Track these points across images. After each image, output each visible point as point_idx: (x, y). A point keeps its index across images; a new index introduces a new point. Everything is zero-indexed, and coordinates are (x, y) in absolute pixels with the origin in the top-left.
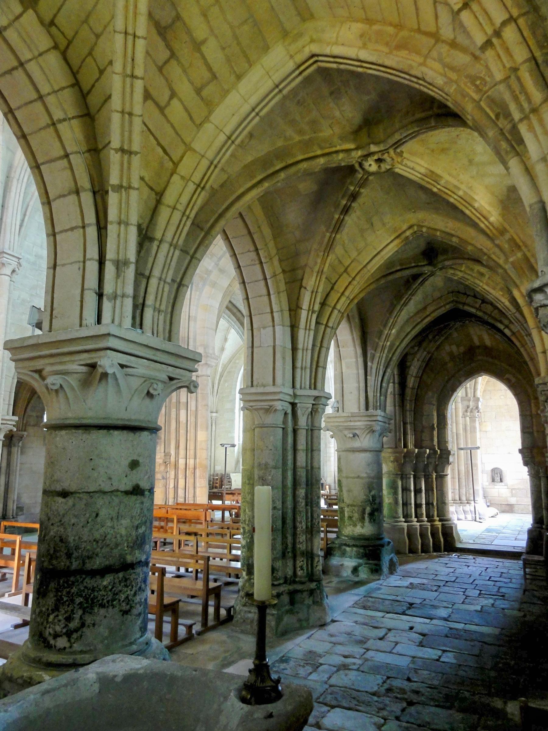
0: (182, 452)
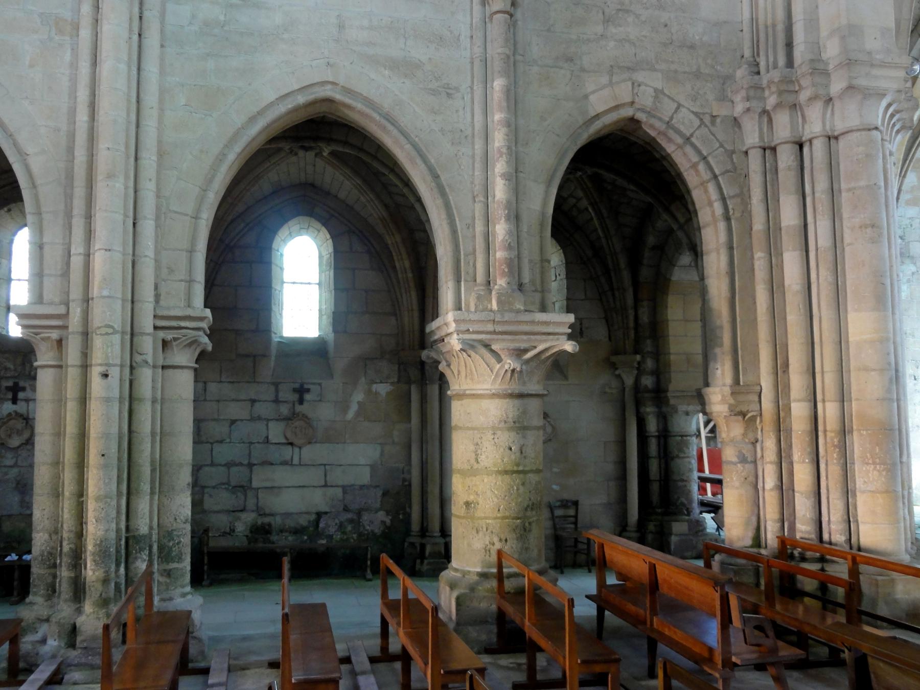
0: (797, 381)
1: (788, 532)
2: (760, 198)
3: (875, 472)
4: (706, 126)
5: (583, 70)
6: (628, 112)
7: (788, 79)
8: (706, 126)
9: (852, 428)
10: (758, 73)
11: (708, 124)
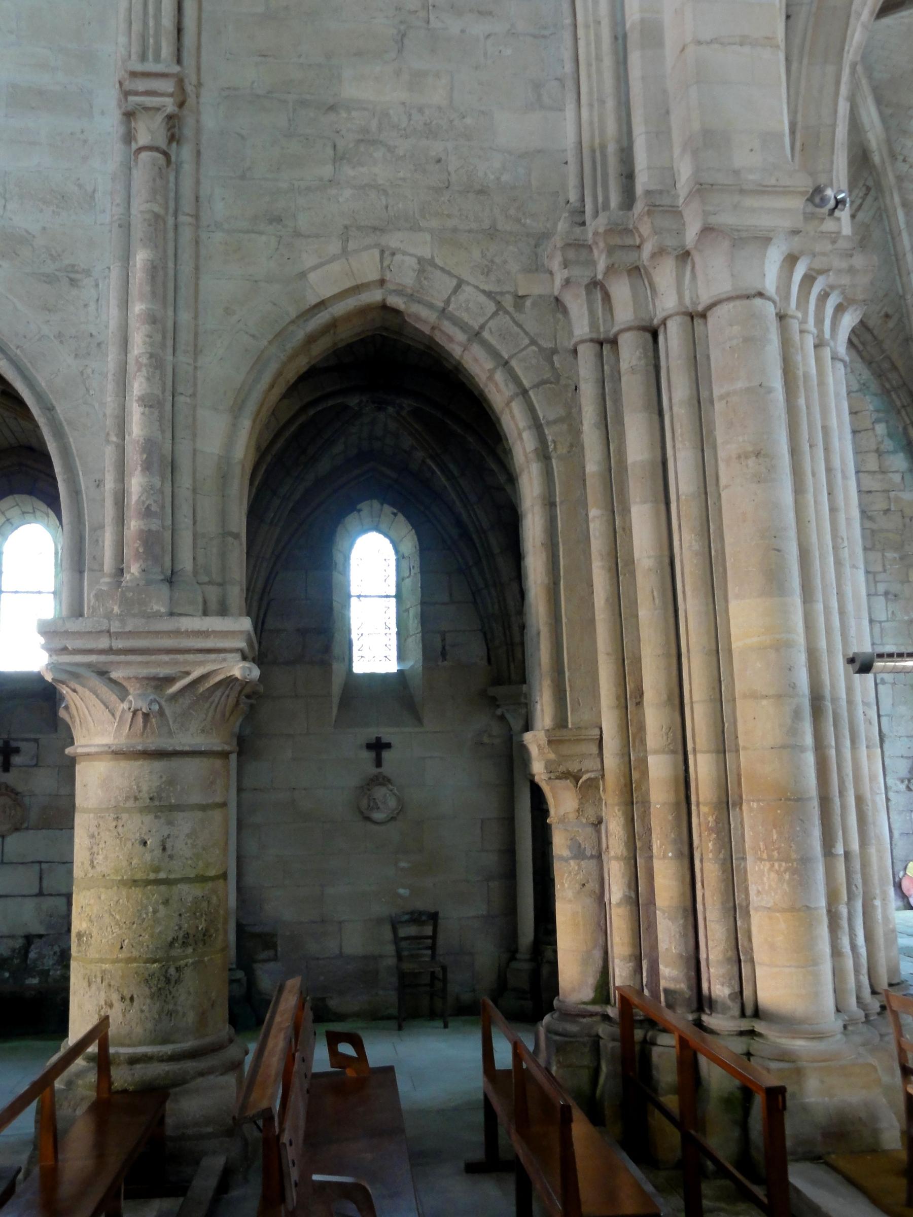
1: (647, 976)
2: (593, 422)
3: (773, 875)
4: (507, 312)
5: (297, 234)
6: (375, 296)
7: (620, 227)
8: (507, 312)
9: (741, 797)
10: (583, 224)
11: (511, 309)
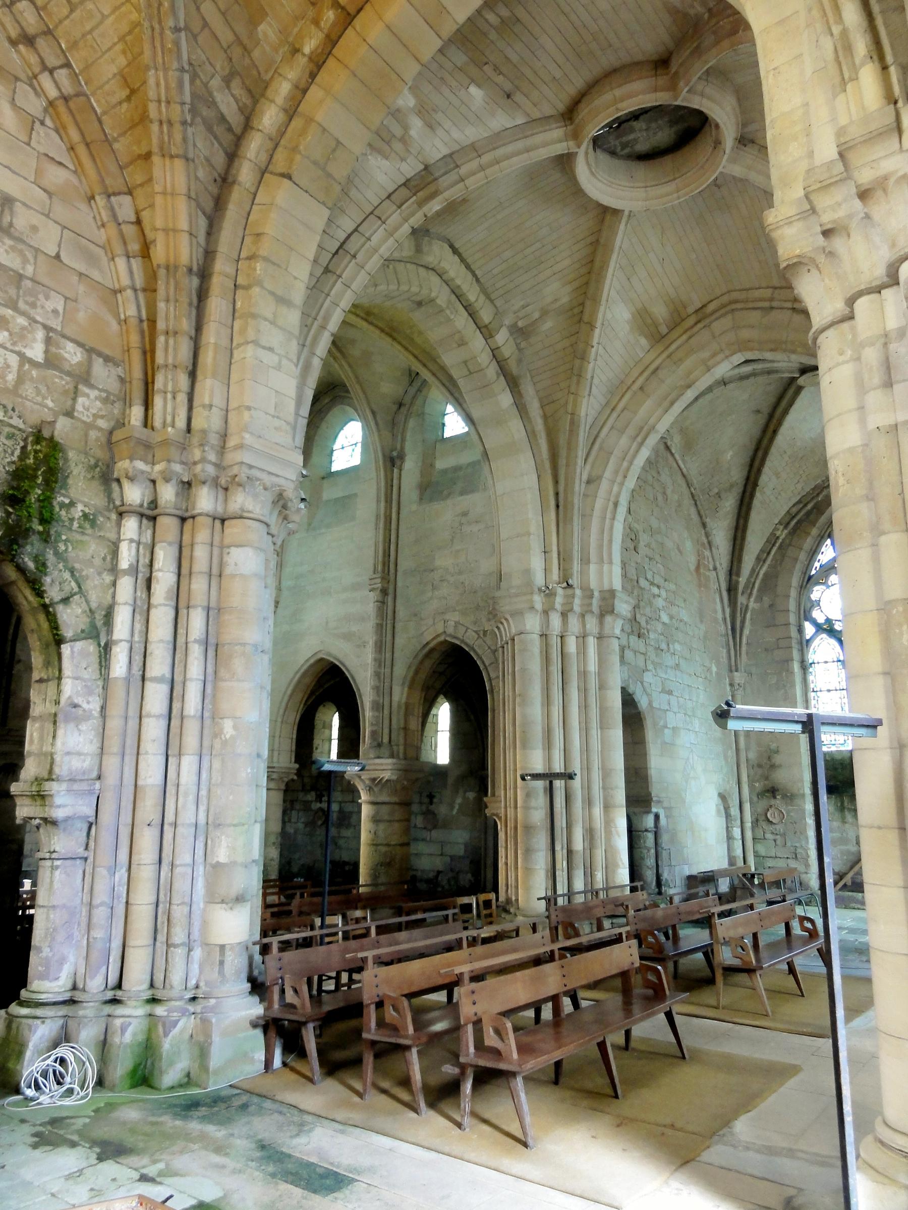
6: (442, 638)
